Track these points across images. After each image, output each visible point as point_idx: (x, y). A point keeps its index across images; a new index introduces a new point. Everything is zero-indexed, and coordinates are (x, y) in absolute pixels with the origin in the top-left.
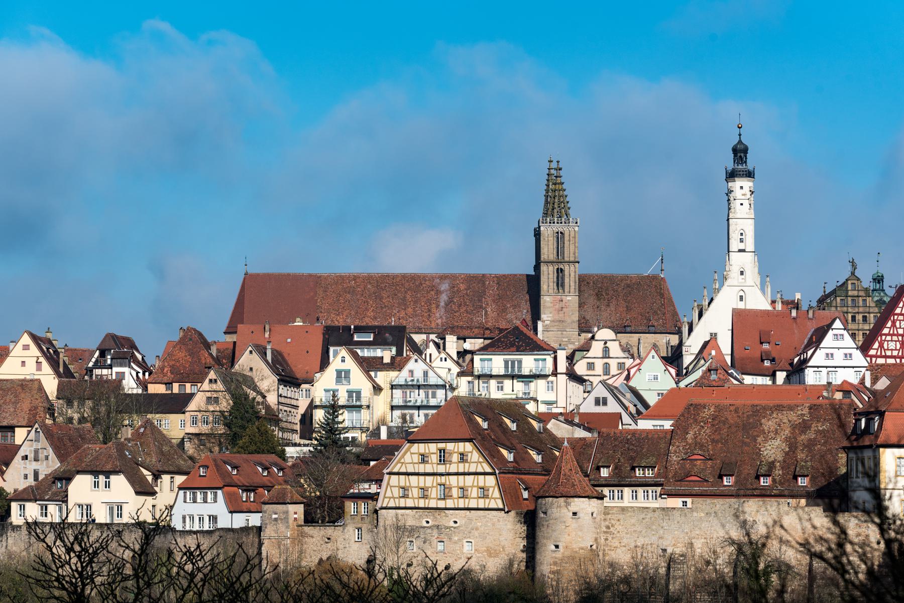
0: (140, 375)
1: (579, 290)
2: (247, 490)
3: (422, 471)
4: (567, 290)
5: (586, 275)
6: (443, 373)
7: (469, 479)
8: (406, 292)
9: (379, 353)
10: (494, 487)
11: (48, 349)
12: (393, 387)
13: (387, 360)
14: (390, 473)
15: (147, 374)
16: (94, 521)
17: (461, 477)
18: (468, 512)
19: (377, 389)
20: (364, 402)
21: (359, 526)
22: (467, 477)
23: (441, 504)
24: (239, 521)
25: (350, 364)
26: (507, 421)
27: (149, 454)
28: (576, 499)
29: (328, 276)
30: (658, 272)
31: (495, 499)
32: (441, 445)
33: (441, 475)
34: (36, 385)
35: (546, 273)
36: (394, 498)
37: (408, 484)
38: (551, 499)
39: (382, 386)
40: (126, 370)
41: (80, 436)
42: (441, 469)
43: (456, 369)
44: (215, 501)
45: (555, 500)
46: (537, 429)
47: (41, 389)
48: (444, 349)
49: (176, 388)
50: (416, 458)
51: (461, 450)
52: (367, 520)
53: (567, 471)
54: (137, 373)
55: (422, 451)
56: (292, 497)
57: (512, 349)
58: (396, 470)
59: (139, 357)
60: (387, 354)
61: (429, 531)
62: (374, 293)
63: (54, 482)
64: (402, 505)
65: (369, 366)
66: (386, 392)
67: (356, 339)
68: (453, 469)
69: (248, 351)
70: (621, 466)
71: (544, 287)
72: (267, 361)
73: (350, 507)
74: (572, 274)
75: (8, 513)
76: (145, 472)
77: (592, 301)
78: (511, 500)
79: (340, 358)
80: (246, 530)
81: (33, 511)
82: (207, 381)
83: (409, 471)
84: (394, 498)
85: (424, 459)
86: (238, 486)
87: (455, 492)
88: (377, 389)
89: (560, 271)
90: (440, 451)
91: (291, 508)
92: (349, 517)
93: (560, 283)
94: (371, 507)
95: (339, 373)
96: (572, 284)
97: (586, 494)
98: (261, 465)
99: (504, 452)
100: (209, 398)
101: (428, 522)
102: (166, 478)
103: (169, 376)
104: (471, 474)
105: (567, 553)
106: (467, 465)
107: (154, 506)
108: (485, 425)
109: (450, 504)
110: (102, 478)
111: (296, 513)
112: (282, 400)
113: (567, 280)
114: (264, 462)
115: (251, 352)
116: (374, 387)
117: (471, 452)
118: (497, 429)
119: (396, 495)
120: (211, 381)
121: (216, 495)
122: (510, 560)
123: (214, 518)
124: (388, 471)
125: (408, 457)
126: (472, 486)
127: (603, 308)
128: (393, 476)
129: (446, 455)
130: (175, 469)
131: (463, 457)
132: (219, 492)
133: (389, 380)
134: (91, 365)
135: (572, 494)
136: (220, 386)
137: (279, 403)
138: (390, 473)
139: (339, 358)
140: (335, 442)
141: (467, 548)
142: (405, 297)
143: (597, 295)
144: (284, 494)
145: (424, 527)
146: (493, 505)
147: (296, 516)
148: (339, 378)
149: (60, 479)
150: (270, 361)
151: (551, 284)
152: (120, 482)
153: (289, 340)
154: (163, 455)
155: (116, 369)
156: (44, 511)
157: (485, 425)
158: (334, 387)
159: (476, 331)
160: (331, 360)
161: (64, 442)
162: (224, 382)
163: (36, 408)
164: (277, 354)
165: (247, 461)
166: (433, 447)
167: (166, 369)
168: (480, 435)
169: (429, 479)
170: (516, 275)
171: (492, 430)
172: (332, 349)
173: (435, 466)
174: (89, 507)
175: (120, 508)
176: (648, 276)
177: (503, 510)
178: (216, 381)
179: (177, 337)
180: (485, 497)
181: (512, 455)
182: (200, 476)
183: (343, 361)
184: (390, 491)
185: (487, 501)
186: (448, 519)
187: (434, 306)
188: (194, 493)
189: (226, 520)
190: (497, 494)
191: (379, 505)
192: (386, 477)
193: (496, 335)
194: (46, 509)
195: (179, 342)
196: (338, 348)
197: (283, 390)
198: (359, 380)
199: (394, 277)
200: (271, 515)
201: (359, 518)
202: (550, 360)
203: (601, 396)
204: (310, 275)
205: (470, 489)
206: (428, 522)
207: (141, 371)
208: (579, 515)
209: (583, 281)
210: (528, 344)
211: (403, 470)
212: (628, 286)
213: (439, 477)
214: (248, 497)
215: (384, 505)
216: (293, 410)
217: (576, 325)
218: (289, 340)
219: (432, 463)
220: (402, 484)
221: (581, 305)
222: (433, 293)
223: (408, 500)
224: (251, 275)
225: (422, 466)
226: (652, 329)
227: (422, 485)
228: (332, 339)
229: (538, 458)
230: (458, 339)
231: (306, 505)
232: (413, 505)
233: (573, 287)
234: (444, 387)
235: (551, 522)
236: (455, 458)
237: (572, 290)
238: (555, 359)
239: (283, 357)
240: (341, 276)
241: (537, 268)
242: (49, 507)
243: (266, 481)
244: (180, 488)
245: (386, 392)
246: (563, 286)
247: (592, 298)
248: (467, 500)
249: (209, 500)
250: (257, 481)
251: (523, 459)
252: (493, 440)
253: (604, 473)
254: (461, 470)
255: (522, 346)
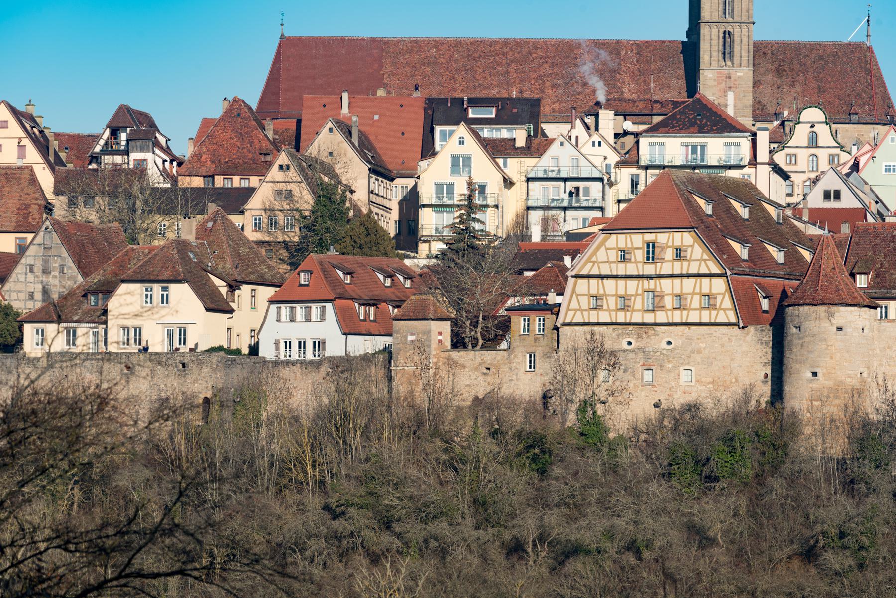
0: (167, 164)
1: (754, 65)
2: (365, 304)
3: (621, 272)
4: (736, 62)
5: (761, 43)
6: (598, 161)
7: (689, 283)
8: (509, 65)
9: (504, 133)
10: (724, 294)
11: (32, 128)
12: (528, 180)
13: (521, 142)
14: (577, 276)
15: (175, 163)
16: (146, 349)
17: (677, 281)
18: (686, 328)
19: (508, 183)
20: (490, 201)
21: (531, 350)
22: (685, 280)
23: (649, 318)
24: (361, 345)
25: (472, 148)
26: (736, 205)
27: (221, 258)
28: (842, 309)
29: (399, 41)
30: (863, 39)
31: (725, 310)
32: (649, 237)
33: (650, 277)
34: (26, 175)
35: (708, 38)
36: (582, 311)
37: (601, 292)
38: (807, 308)
39: (514, 179)
40: (148, 156)
41: (106, 240)
42: (649, 269)
43: (614, 158)
44: (323, 319)
45: (813, 308)
46: (775, 218)
47: (33, 180)
48: (597, 129)
49: (219, 181)
50: (614, 256)
51: (678, 243)
52: (543, 342)
53: (828, 270)
54: (164, 161)
55: (622, 245)
56: (435, 312)
57: (692, 129)
58: (584, 272)
59: (162, 141)
60: (520, 135)
61: (632, 355)
62: (464, 66)
63: (85, 295)
64: (594, 320)
65: (497, 150)
66: (520, 186)
67: (471, 115)
68: (666, 269)
69: (326, 130)
70: (884, 273)
71: (705, 57)
72: (354, 146)
73: (519, 323)
74: (745, 40)
75: (20, 340)
76: (217, 282)
77: (769, 78)
78: (747, 314)
79: (454, 141)
80: (367, 359)
81: (55, 338)
82: (275, 167)
83: (604, 273)
84: (582, 311)
85: (624, 256)
86: (353, 299)
87: (668, 302)
88: (508, 183)
89: (727, 35)
90: (648, 246)
91: (435, 326)
92: (517, 338)
93: (727, 53)
94: (549, 324)
95: (455, 159)
96: (745, 54)
97: (855, 302)
98: (382, 271)
99: (736, 246)
100: (279, 192)
101: (630, 343)
102: (246, 289)
103: (210, 167)
104: (692, 275)
105: (829, 383)
106: (685, 264)
107: (229, 329)
108: (708, 209)
109: (661, 317)
110: (157, 288)
111: (440, 334)
112: (374, 198)
113: (737, 48)
114: (385, 267)
115: (331, 130)
116: (505, 180)
117: (692, 246)
118: (724, 216)
119: (585, 306)
120: (281, 167)
121: (323, 309)
122: (745, 393)
123: (319, 344)
124: (574, 273)
125: (603, 254)
126: (693, 293)
127: (786, 88)
128: (580, 281)
129: (657, 251)
130: (259, 279)
131: (679, 254)
132: (329, 307)
133: (523, 170)
134: (98, 149)
135: (837, 302)
136: (293, 174)
137: (371, 202)
138: (577, 276)
139: (456, 138)
140: (473, 247)
141: (685, 376)
142: (507, 72)
143: (777, 70)
144: (425, 307)
145: (624, 351)
146: (722, 319)
147: (440, 338)
148: (454, 164)
149: (95, 293)
150: (357, 144)
151: (715, 54)
152: (183, 295)
153: (376, 118)
154: (240, 259)
155: (135, 156)
156: (72, 336)
157: (708, 209)
158: (449, 179)
159: (641, 105)
160: (437, 147)
161: (83, 247)
162: (302, 170)
163: (28, 207)
164: (363, 136)
165: (363, 265)
166: (637, 240)
167: (204, 157)
168: (703, 222)
169: (632, 283)
170: (663, 42)
171: (719, 218)
172: (438, 129)
173: (640, 265)
174: (138, 331)
175: (183, 332)
176: (849, 44)
177: (737, 325)
178: (288, 167)
179: (216, 112)
180: (711, 307)
181: (746, 251)
182: (301, 285)
183: (461, 143)
184: (575, 301)
185: (714, 313)
186: (658, 341)
187: (548, 84)
188: (292, 308)
189: (337, 345)
190: (727, 303)
191: (561, 320)
192: (571, 281)
193: (669, 110)
194: (74, 335)
195: (222, 119)
196: (448, 129)
197: (378, 185)
198: (483, 169)
199: (492, 43)
200: (406, 337)
201: (531, 338)
202: (745, 144)
203: (832, 188)
204: (373, 40)
205: (689, 297)
206: (630, 343)
207: (168, 159)
208: (848, 330)
209: (760, 50)
210: (715, 124)
211: (595, 272)
212: (821, 58)
213: (645, 281)
214: (367, 315)
215: (568, 321)
216: (385, 214)
217: (749, 112)
218: (376, 118)
219: (636, 262)
220: (594, 291)
221: (756, 84)
222: (546, 65)
223: (601, 313)
224: (289, 39)
225: (622, 265)
226: (854, 118)
227: (621, 292)
228: (437, 116)
229: (779, 256)
230: (616, 115)
231: (455, 323)
232: (609, 321)
233: (745, 58)
234: (601, 180)
235: (807, 339)
236: (669, 254)
237: (744, 62)
238: (754, 143)
239: (369, 141)
240: (416, 42)
241: (694, 29)
242: (80, 332)
243: (390, 294)
244: (271, 302)
245: (520, 186)
246: (731, 57)
247: (770, 75)
248: (685, 313)
249: (313, 318)
250: (378, 293)
251: (760, 258)
252: (721, 230)
253: (862, 281)
254: (677, 271)
255: (707, 126)
